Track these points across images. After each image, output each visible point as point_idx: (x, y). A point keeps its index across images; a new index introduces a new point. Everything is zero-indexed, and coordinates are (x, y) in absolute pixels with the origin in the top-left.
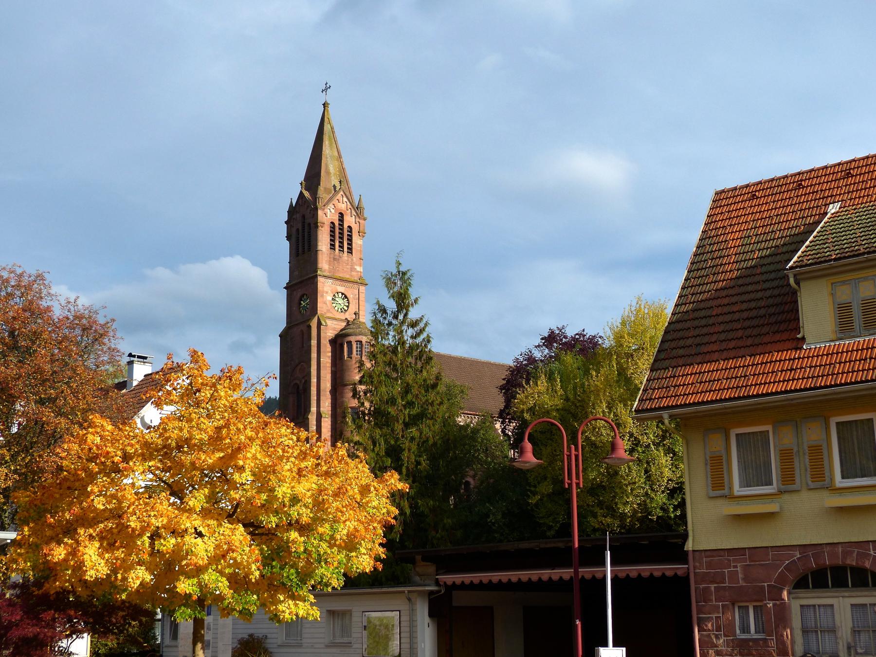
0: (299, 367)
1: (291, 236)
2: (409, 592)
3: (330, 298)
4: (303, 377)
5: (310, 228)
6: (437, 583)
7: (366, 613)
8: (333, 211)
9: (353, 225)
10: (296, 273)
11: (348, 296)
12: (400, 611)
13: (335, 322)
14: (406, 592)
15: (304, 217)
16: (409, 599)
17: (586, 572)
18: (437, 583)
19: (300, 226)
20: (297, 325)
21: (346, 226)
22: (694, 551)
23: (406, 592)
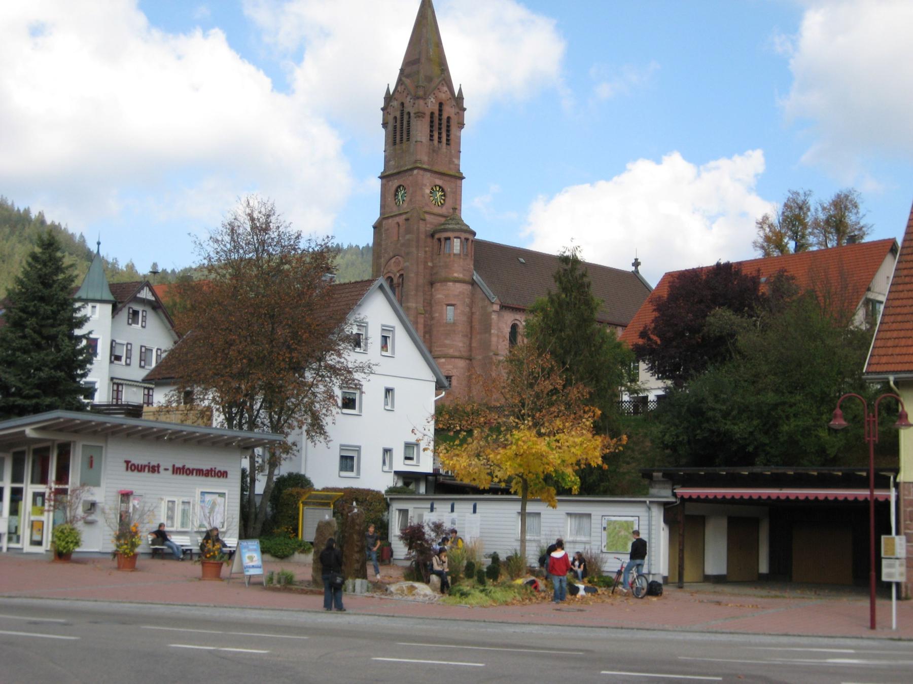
0: (393, 260)
1: (387, 123)
2: (650, 502)
3: (428, 191)
4: (398, 271)
5: (409, 117)
6: (675, 495)
7: (606, 517)
8: (434, 101)
9: (453, 116)
10: (392, 163)
11: (445, 189)
12: (639, 517)
13: (432, 216)
14: (648, 502)
15: (402, 104)
16: (649, 508)
17: (879, 493)
18: (675, 495)
19: (398, 115)
20: (392, 217)
21: (445, 116)
22: (905, 483)
23: (648, 502)
